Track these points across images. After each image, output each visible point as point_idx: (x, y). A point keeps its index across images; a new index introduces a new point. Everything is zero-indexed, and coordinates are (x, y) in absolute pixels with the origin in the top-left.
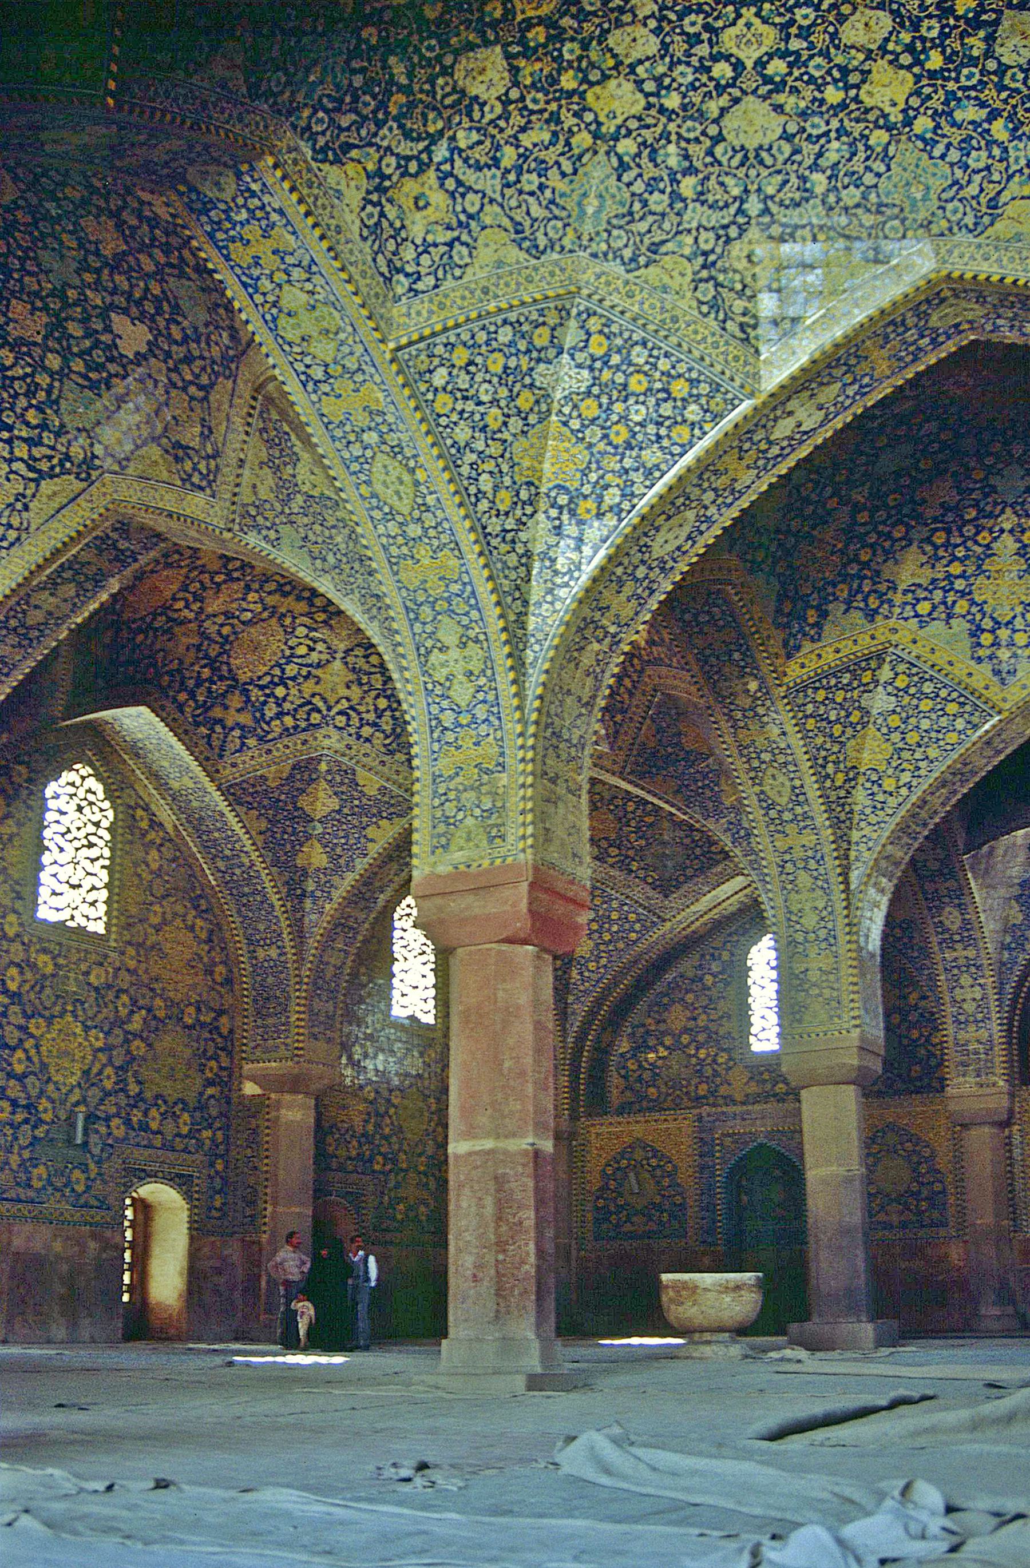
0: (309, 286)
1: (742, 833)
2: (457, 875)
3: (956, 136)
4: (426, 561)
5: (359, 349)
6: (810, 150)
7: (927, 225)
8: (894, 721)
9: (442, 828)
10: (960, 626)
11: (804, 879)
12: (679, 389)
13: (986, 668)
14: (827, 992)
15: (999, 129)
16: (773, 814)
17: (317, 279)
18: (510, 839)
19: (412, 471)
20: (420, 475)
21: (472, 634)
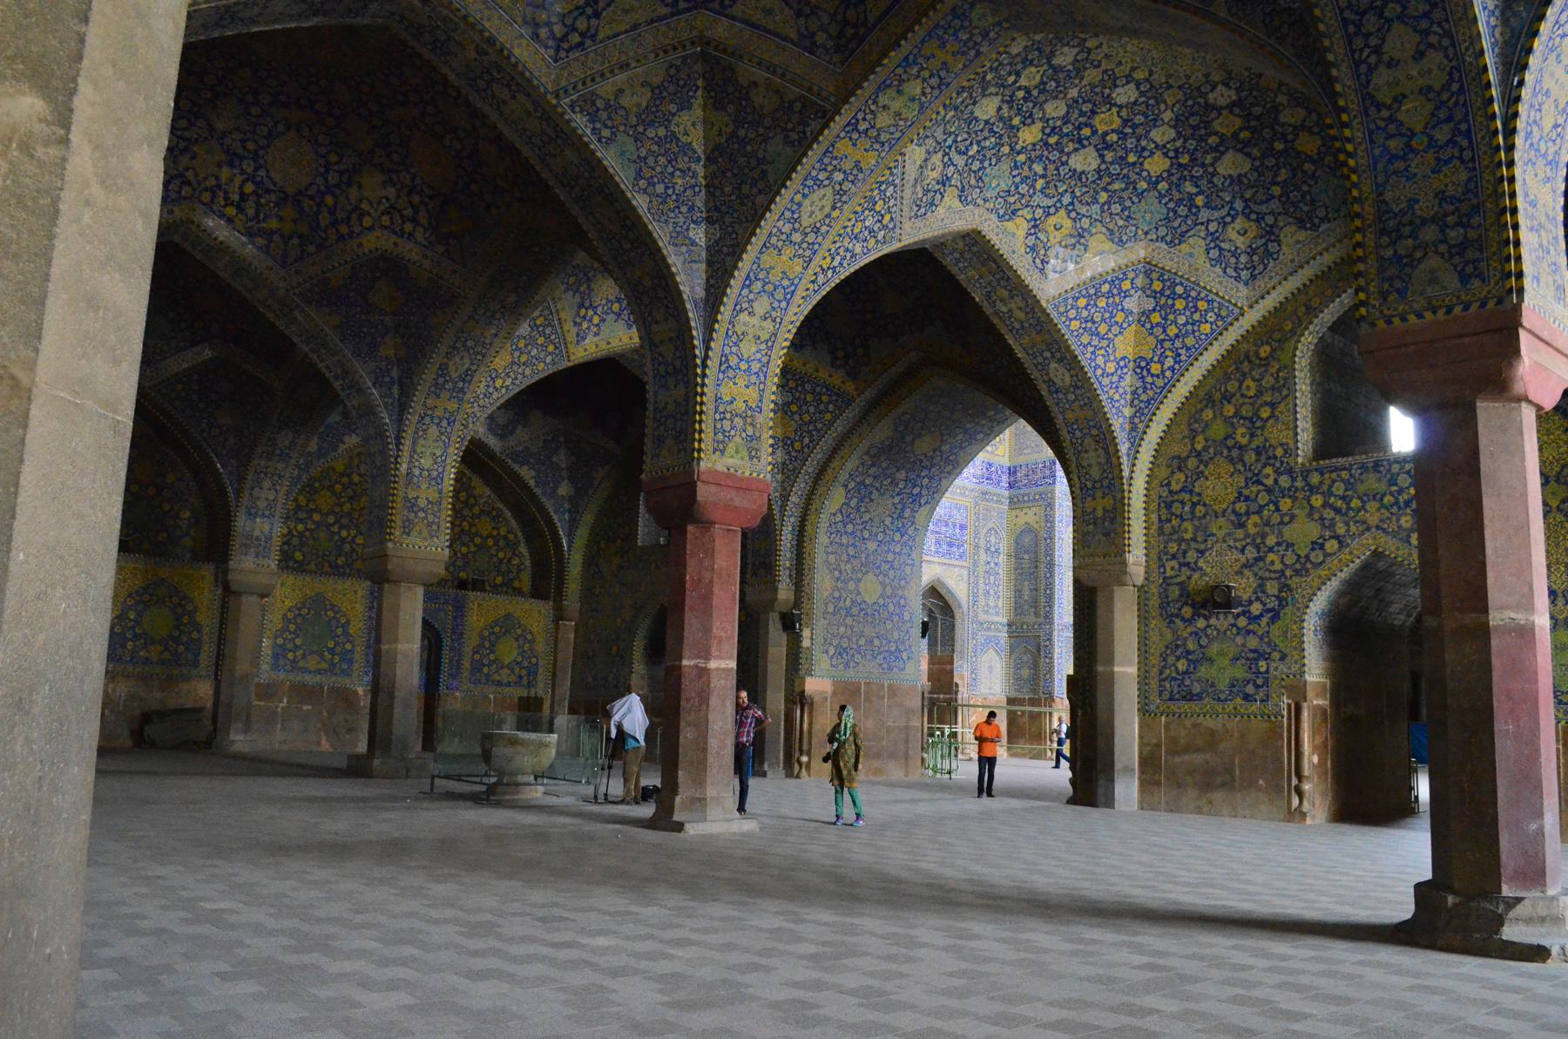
0: (928, 90)
1: (387, 379)
2: (728, 476)
3: (1026, 172)
4: (784, 258)
5: (898, 135)
6: (986, 133)
7: (985, 201)
8: (521, 344)
9: (720, 437)
10: (577, 299)
11: (433, 431)
12: (887, 217)
13: (574, 330)
14: (431, 518)
15: (1040, 184)
16: (441, 380)
17: (936, 92)
18: (763, 462)
19: (834, 208)
20: (835, 214)
21: (774, 314)
